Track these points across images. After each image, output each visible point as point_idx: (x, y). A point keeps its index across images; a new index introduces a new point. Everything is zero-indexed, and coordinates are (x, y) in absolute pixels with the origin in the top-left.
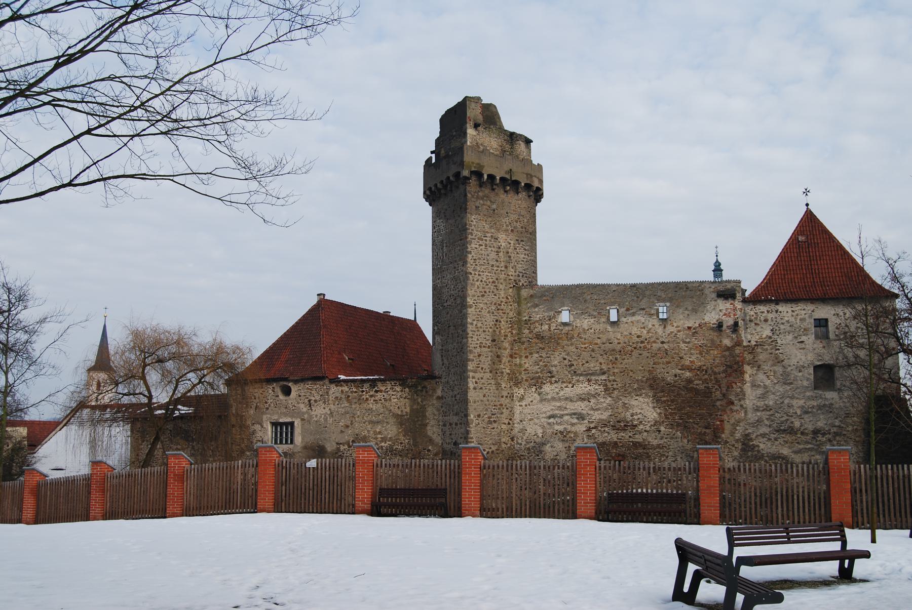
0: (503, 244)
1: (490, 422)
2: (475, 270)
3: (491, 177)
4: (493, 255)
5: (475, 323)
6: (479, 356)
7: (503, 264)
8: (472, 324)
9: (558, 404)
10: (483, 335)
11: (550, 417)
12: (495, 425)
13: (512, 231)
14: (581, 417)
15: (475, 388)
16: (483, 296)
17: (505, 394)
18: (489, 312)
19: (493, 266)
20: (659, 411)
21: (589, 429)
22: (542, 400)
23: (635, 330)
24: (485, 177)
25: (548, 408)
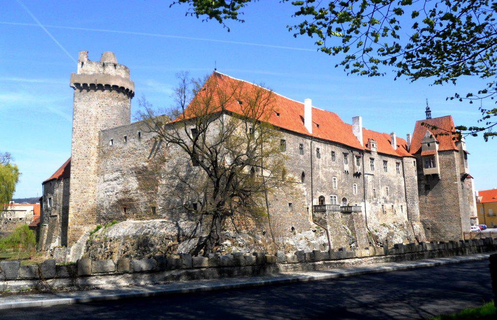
0: (94, 113)
1: (82, 193)
2: (77, 126)
3: (85, 85)
4: (88, 119)
5: (76, 149)
6: (78, 163)
7: (94, 122)
8: (74, 150)
9: (108, 183)
10: (80, 154)
11: (106, 189)
12: (85, 194)
13: (100, 107)
14: (114, 188)
15: (74, 178)
16: (81, 137)
17: (92, 180)
18: (84, 144)
19: (87, 123)
20: (138, 183)
21: (116, 194)
22: (105, 181)
23: (131, 145)
24: (81, 85)
25: (105, 184)
